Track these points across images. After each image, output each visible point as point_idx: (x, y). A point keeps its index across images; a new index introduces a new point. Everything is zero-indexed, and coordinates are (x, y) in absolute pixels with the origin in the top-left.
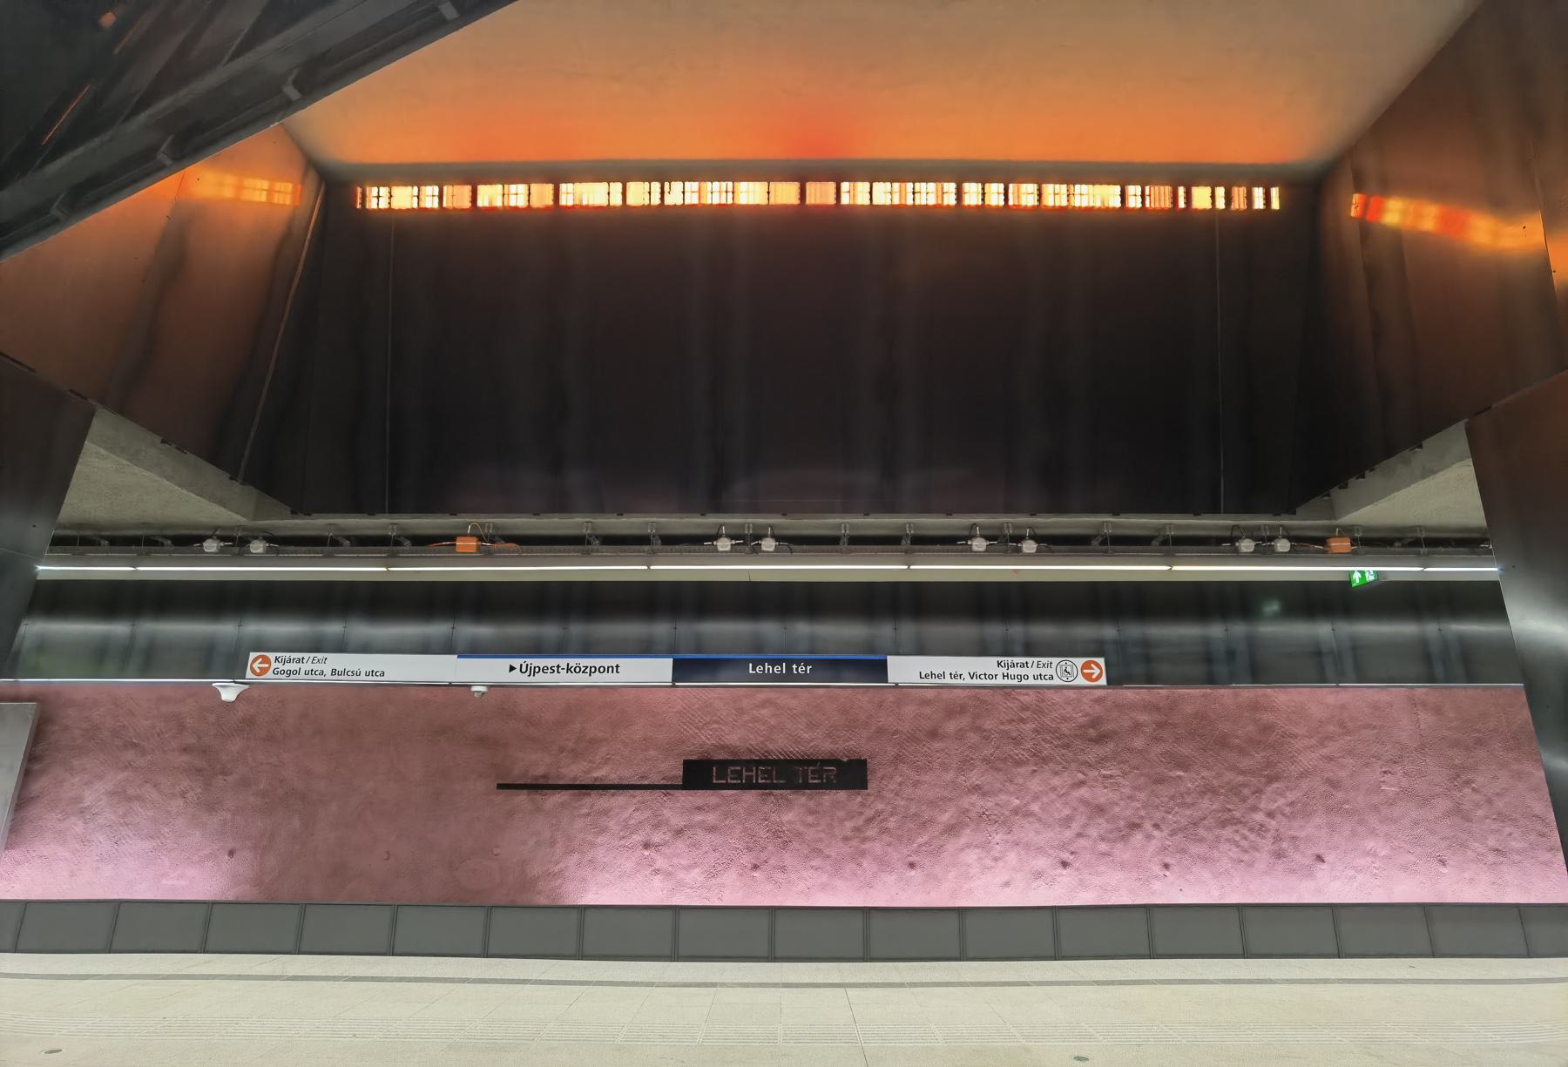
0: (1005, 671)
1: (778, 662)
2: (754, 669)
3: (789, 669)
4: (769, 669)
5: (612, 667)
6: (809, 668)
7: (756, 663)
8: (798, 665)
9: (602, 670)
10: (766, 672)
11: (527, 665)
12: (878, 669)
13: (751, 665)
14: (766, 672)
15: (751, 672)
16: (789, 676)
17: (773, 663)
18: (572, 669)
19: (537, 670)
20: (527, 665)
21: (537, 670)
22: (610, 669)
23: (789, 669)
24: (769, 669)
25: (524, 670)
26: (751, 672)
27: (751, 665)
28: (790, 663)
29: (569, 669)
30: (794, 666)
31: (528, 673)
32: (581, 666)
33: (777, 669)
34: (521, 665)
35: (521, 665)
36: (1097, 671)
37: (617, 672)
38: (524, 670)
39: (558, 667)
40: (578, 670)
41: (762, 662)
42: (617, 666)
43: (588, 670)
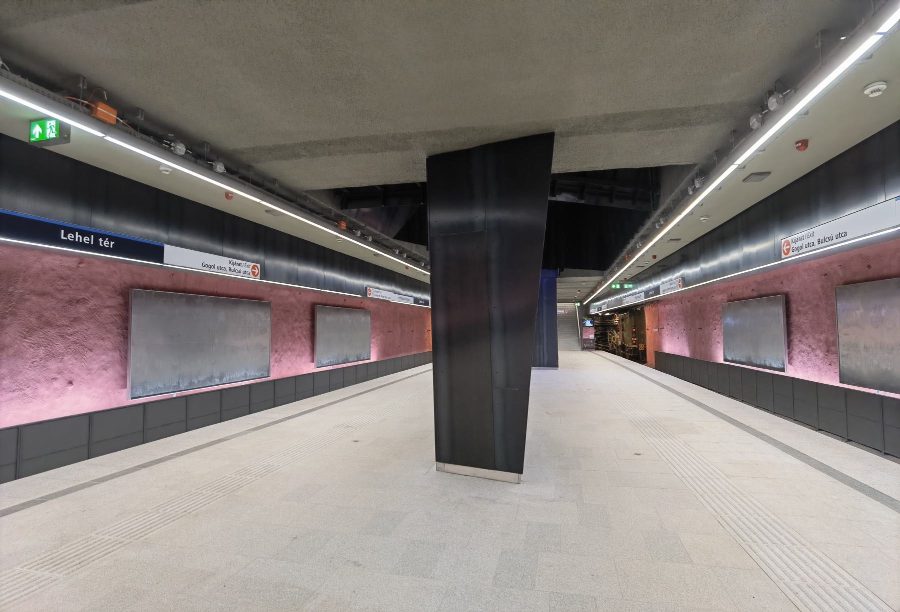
0: (231, 266)
1: (88, 234)
2: (65, 235)
3: (96, 241)
4: (79, 238)
6: (112, 243)
7: (68, 230)
8: (104, 240)
10: (77, 240)
12: (156, 253)
13: (63, 231)
14: (77, 240)
15: (62, 237)
16: (96, 247)
17: (83, 233)
23: (96, 241)
24: (79, 238)
26: (62, 237)
27: (63, 231)
28: (97, 236)
30: (101, 240)
33: (86, 239)
36: (257, 271)
41: (73, 231)
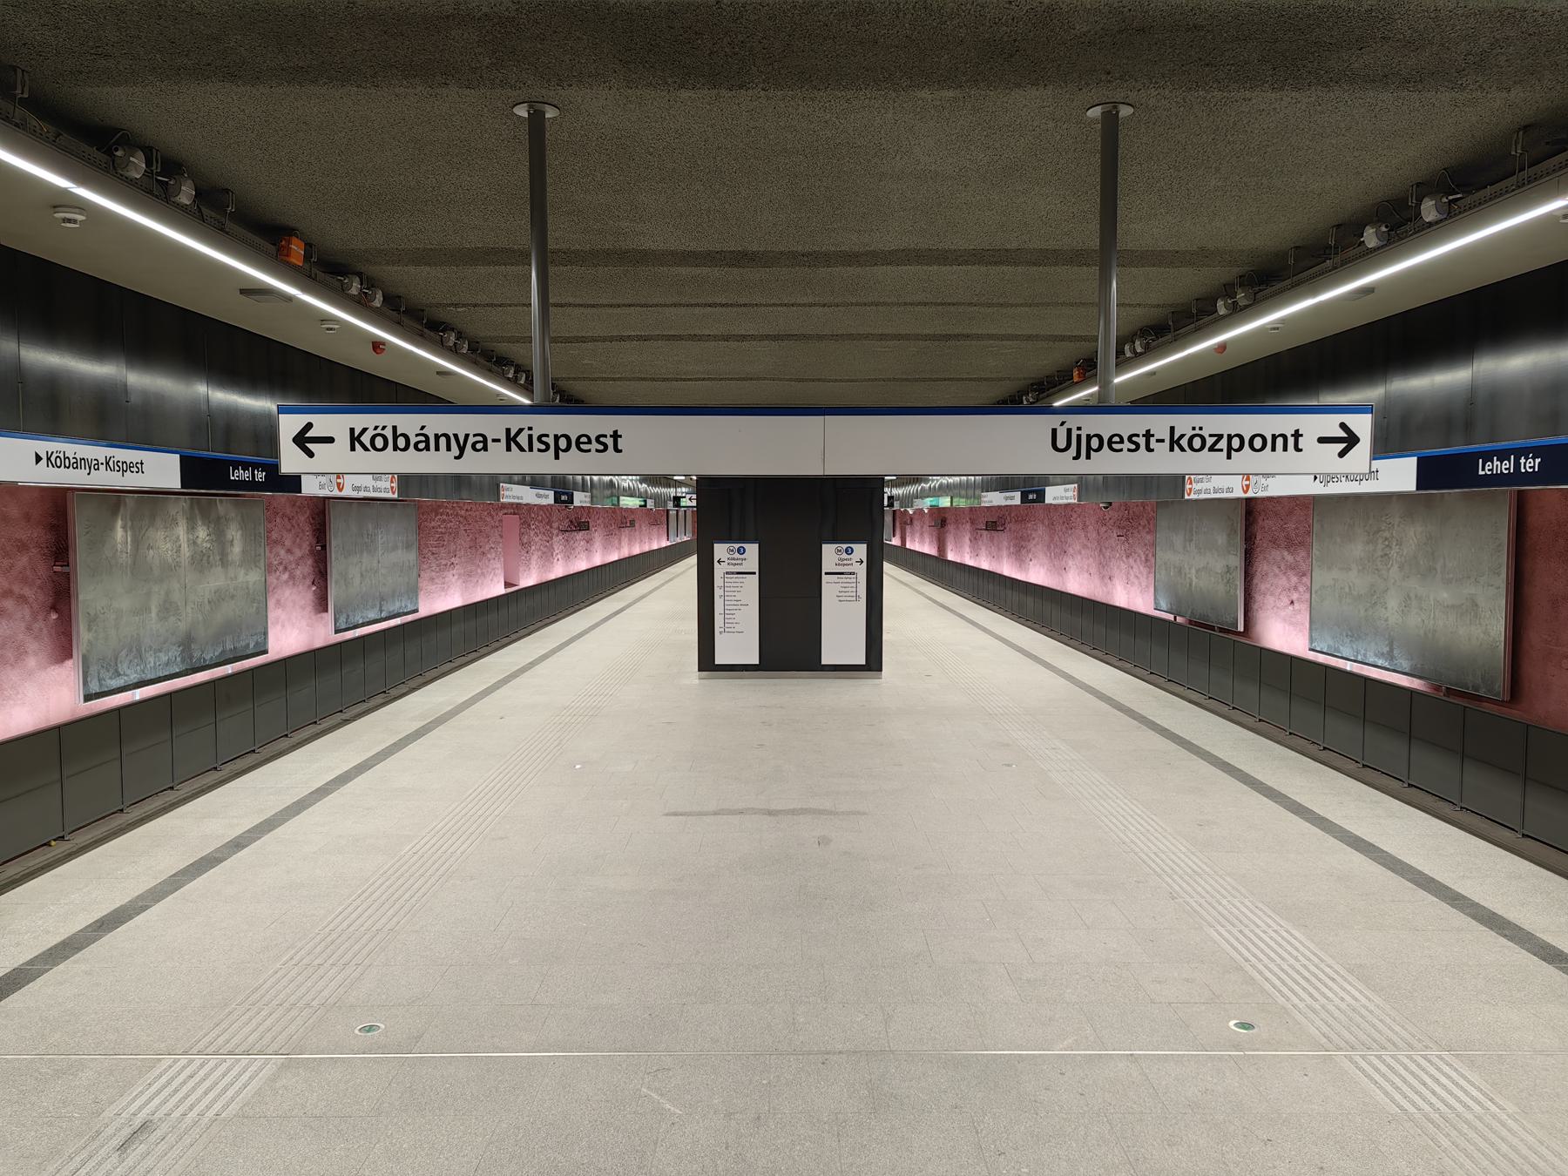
5: (1284, 437)
9: (1258, 443)
11: (1069, 431)
18: (1184, 442)
19: (1095, 443)
20: (1069, 431)
21: (1095, 443)
22: (1280, 441)
25: (1062, 443)
29: (1174, 443)
31: (1073, 451)
32: (1205, 433)
34: (1054, 431)
35: (1054, 431)
37: (1297, 449)
38: (1062, 443)
39: (1148, 435)
40: (1197, 443)
42: (1297, 435)
43: (1223, 444)
